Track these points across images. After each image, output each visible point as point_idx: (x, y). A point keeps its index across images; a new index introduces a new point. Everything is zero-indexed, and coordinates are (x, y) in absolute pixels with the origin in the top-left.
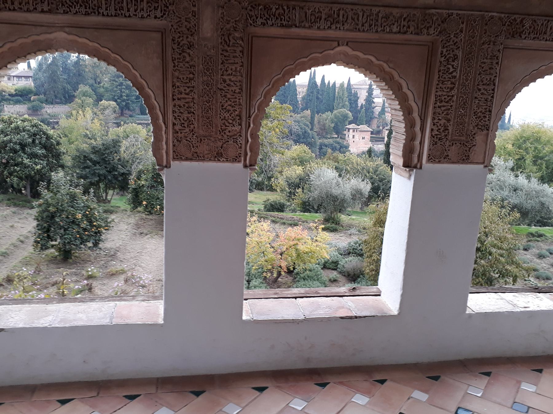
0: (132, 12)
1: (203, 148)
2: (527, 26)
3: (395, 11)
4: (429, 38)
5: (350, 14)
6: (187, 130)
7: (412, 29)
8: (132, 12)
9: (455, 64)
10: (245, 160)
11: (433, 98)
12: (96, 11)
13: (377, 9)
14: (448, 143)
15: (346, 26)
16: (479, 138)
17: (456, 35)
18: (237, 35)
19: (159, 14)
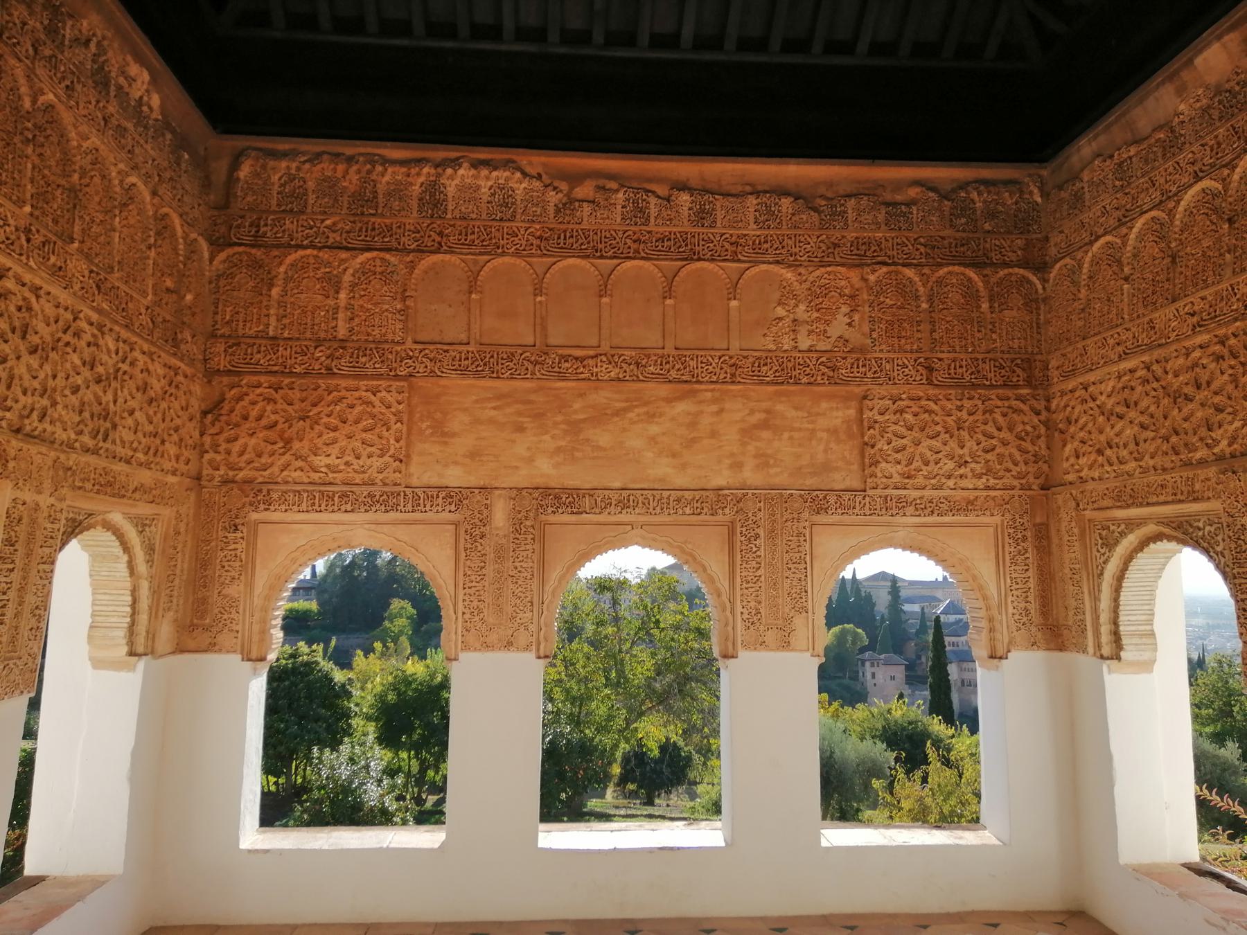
0: (428, 507)
1: (493, 638)
2: (832, 501)
3: (686, 494)
4: (727, 518)
5: (641, 499)
6: (477, 618)
7: (706, 510)
8: (428, 507)
9: (757, 542)
10: (538, 650)
11: (739, 580)
12: (395, 508)
13: (668, 493)
14: (762, 628)
15: (637, 511)
16: (799, 621)
17: (754, 514)
18: (528, 523)
19: (453, 508)
